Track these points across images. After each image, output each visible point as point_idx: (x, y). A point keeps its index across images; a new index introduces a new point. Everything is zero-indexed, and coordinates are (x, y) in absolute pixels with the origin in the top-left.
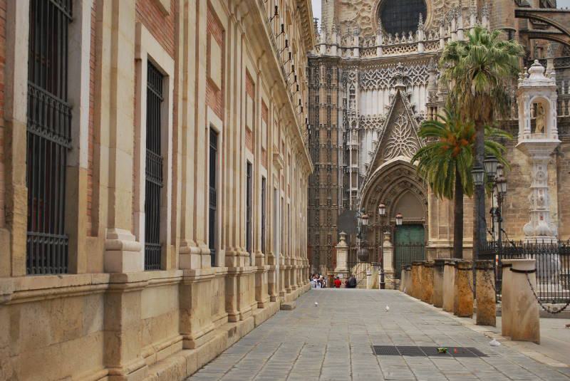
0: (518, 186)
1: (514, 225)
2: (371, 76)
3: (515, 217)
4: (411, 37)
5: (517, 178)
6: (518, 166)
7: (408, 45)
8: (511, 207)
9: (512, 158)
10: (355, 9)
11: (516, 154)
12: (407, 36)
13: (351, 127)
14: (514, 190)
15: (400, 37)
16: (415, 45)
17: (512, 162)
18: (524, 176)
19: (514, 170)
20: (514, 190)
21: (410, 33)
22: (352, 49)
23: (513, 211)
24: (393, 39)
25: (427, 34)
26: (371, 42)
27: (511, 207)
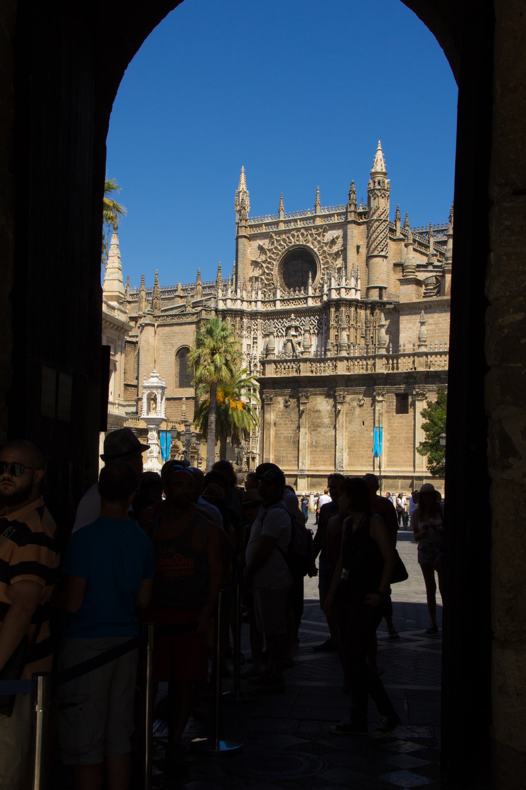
0: (319, 427)
1: (315, 458)
2: (280, 324)
3: (316, 451)
4: (302, 292)
5: (319, 421)
6: (320, 412)
7: (300, 299)
8: (314, 443)
9: (316, 405)
10: (262, 266)
11: (319, 402)
12: (300, 291)
13: (252, 369)
14: (316, 430)
15: (295, 291)
16: (306, 299)
17: (316, 408)
18: (324, 420)
19: (316, 414)
20: (316, 430)
21: (302, 288)
22: (256, 302)
23: (316, 447)
24: (289, 293)
25: (315, 290)
26: (272, 296)
27: (314, 443)
